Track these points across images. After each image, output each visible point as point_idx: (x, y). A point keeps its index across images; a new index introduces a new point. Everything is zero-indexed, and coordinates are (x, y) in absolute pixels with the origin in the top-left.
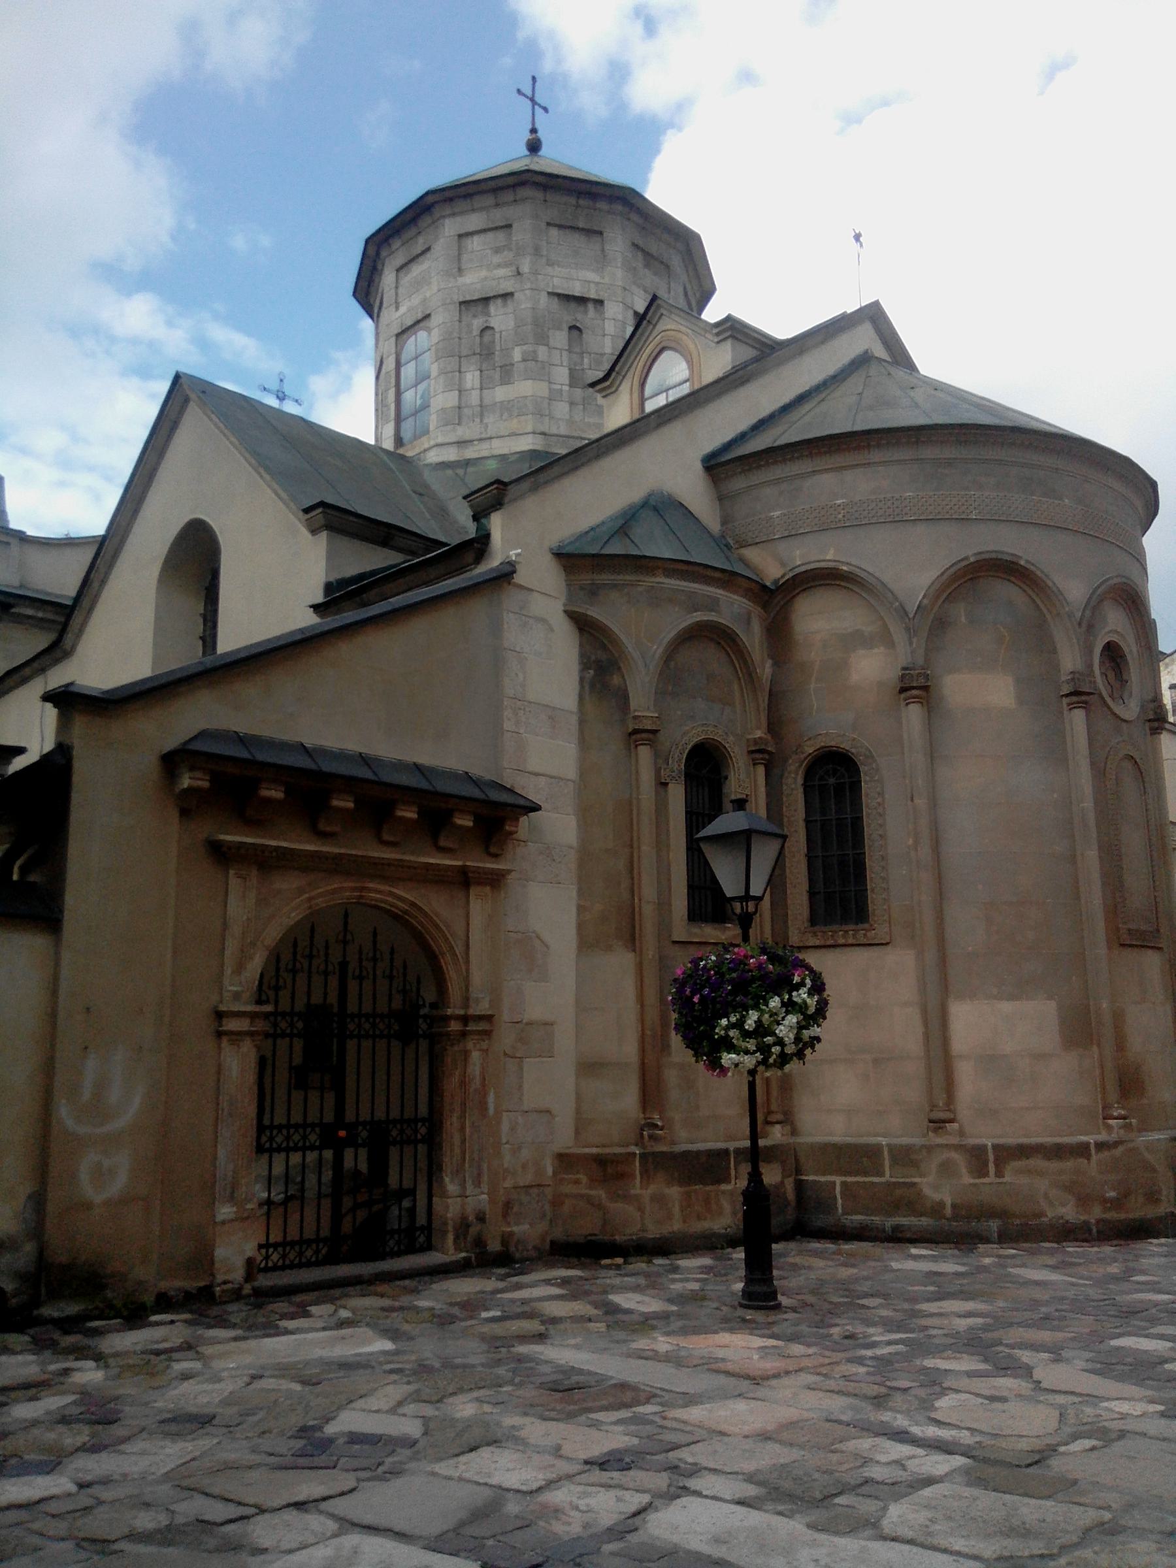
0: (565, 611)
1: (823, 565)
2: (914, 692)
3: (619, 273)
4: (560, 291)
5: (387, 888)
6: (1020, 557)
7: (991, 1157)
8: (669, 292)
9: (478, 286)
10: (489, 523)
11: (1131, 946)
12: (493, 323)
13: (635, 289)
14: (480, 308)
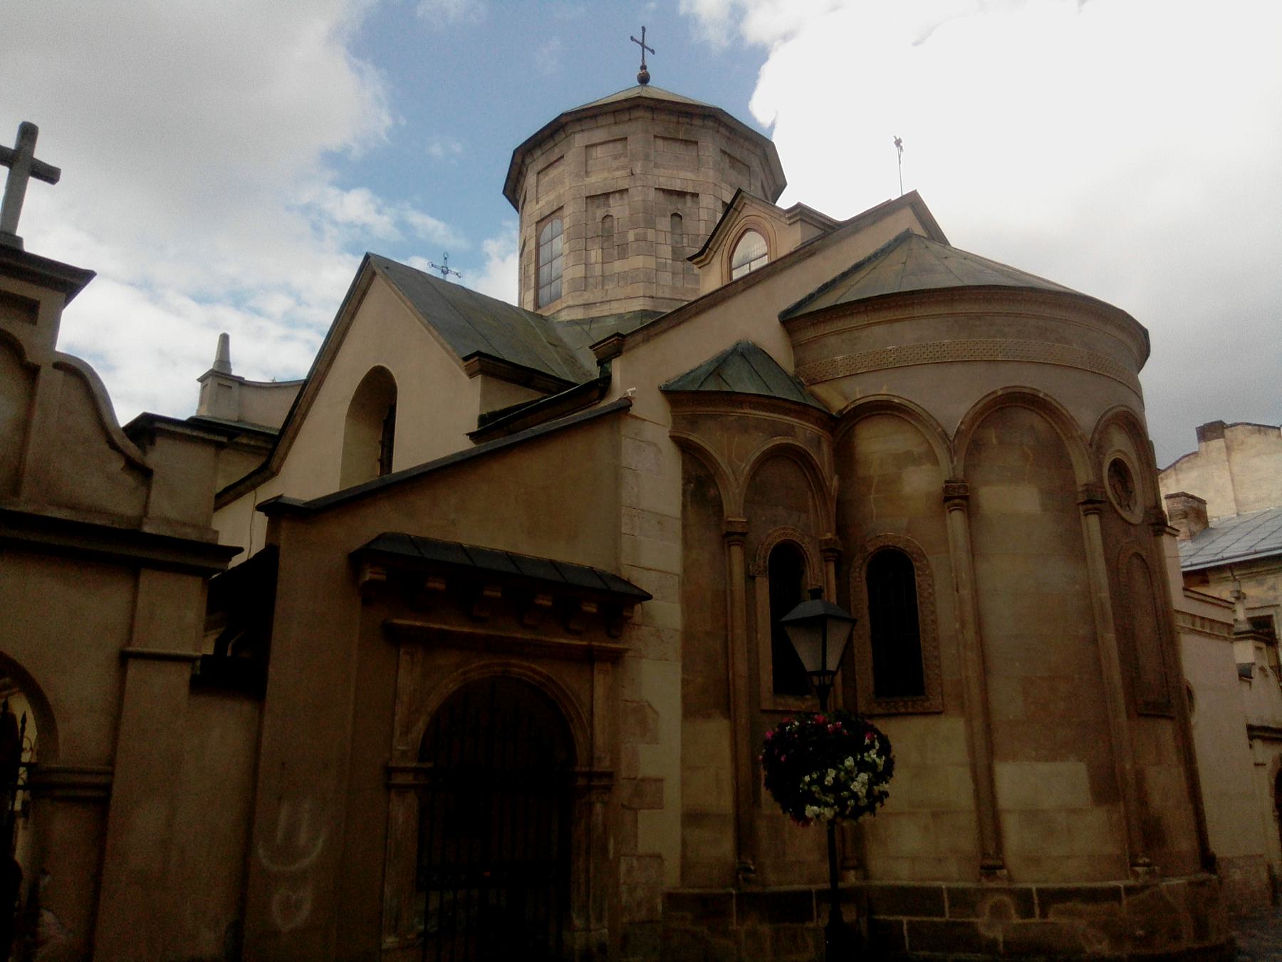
0: (670, 436)
1: (878, 398)
2: (957, 501)
3: (711, 173)
4: (666, 188)
5: (527, 664)
6: (1039, 391)
7: (1036, 901)
8: (750, 187)
10: (611, 367)
11: (1147, 715)
12: (613, 212)
13: (724, 185)
14: (602, 200)
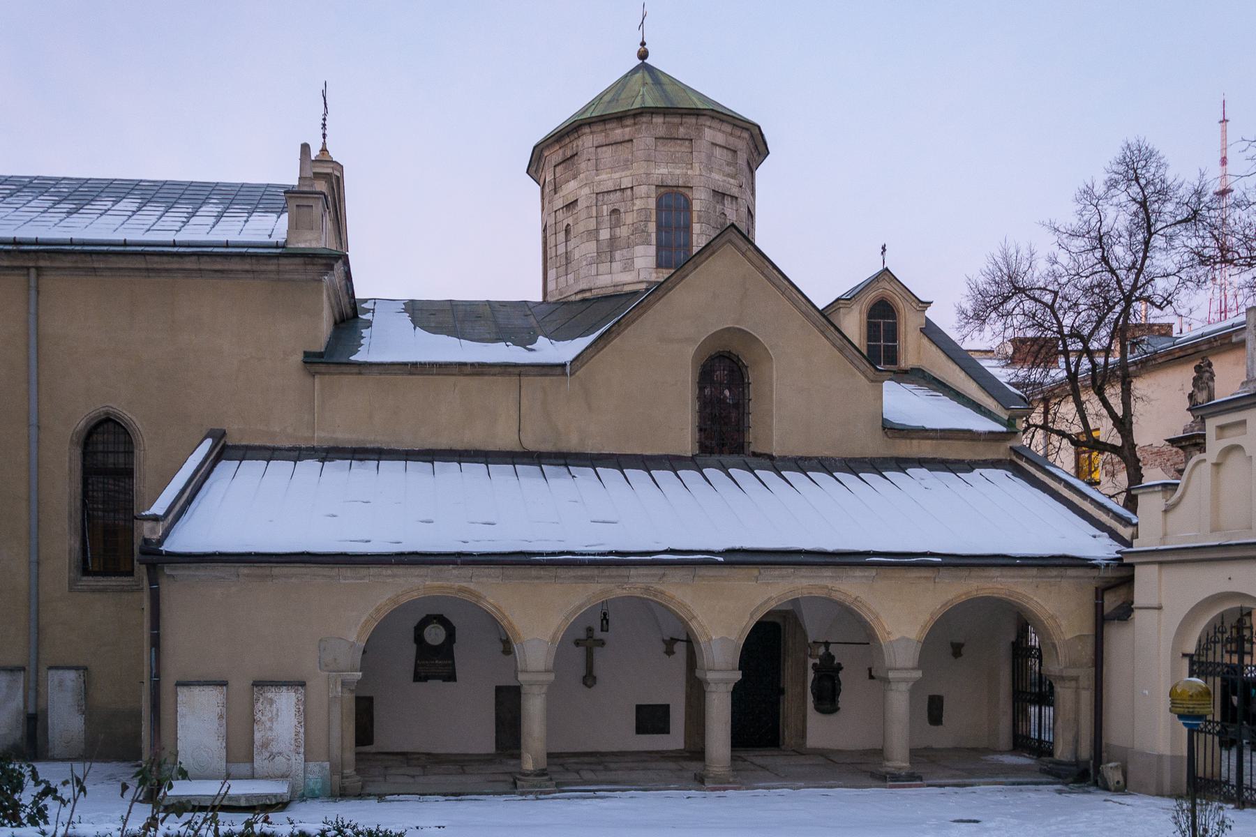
9: (722, 183)
